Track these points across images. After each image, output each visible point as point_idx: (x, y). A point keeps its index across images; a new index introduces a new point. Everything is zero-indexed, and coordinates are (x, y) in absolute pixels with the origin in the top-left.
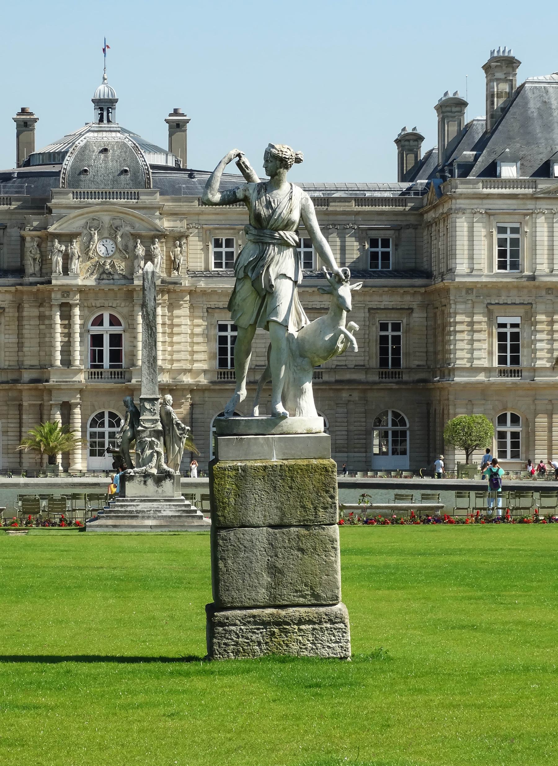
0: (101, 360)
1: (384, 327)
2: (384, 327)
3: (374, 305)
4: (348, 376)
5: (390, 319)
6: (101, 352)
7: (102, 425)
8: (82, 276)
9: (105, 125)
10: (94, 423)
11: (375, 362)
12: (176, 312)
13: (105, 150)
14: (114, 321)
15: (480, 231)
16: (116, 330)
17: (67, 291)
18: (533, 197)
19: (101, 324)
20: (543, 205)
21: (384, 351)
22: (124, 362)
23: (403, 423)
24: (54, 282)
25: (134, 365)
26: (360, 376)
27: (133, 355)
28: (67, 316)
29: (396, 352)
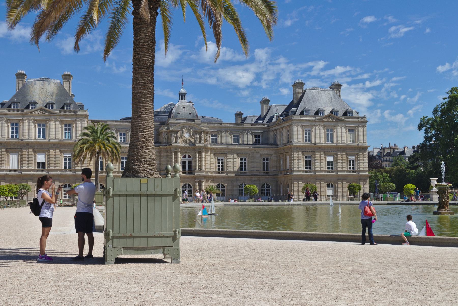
0: (185, 168)
1: (264, 159)
2: (264, 159)
3: (261, 153)
4: (254, 173)
5: (266, 157)
6: (185, 166)
7: (222, 188)
8: (181, 143)
9: (183, 100)
10: (262, 187)
11: (262, 169)
12: (207, 154)
13: (184, 107)
14: (189, 157)
15: (300, 130)
16: (190, 159)
17: (176, 148)
18: (315, 121)
19: (185, 157)
20: (317, 124)
21: (264, 166)
22: (192, 169)
23: (269, 187)
24: (172, 145)
25: (195, 169)
26: (258, 173)
27: (195, 167)
28: (176, 155)
29: (267, 166)
